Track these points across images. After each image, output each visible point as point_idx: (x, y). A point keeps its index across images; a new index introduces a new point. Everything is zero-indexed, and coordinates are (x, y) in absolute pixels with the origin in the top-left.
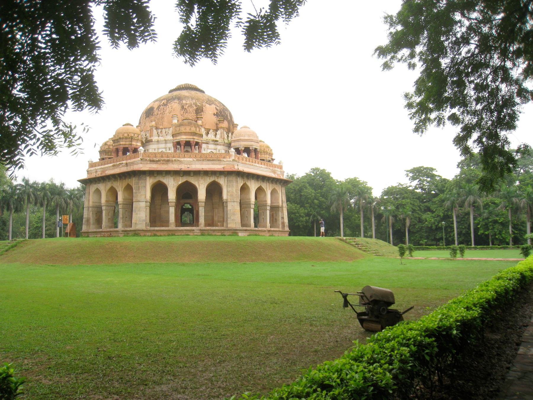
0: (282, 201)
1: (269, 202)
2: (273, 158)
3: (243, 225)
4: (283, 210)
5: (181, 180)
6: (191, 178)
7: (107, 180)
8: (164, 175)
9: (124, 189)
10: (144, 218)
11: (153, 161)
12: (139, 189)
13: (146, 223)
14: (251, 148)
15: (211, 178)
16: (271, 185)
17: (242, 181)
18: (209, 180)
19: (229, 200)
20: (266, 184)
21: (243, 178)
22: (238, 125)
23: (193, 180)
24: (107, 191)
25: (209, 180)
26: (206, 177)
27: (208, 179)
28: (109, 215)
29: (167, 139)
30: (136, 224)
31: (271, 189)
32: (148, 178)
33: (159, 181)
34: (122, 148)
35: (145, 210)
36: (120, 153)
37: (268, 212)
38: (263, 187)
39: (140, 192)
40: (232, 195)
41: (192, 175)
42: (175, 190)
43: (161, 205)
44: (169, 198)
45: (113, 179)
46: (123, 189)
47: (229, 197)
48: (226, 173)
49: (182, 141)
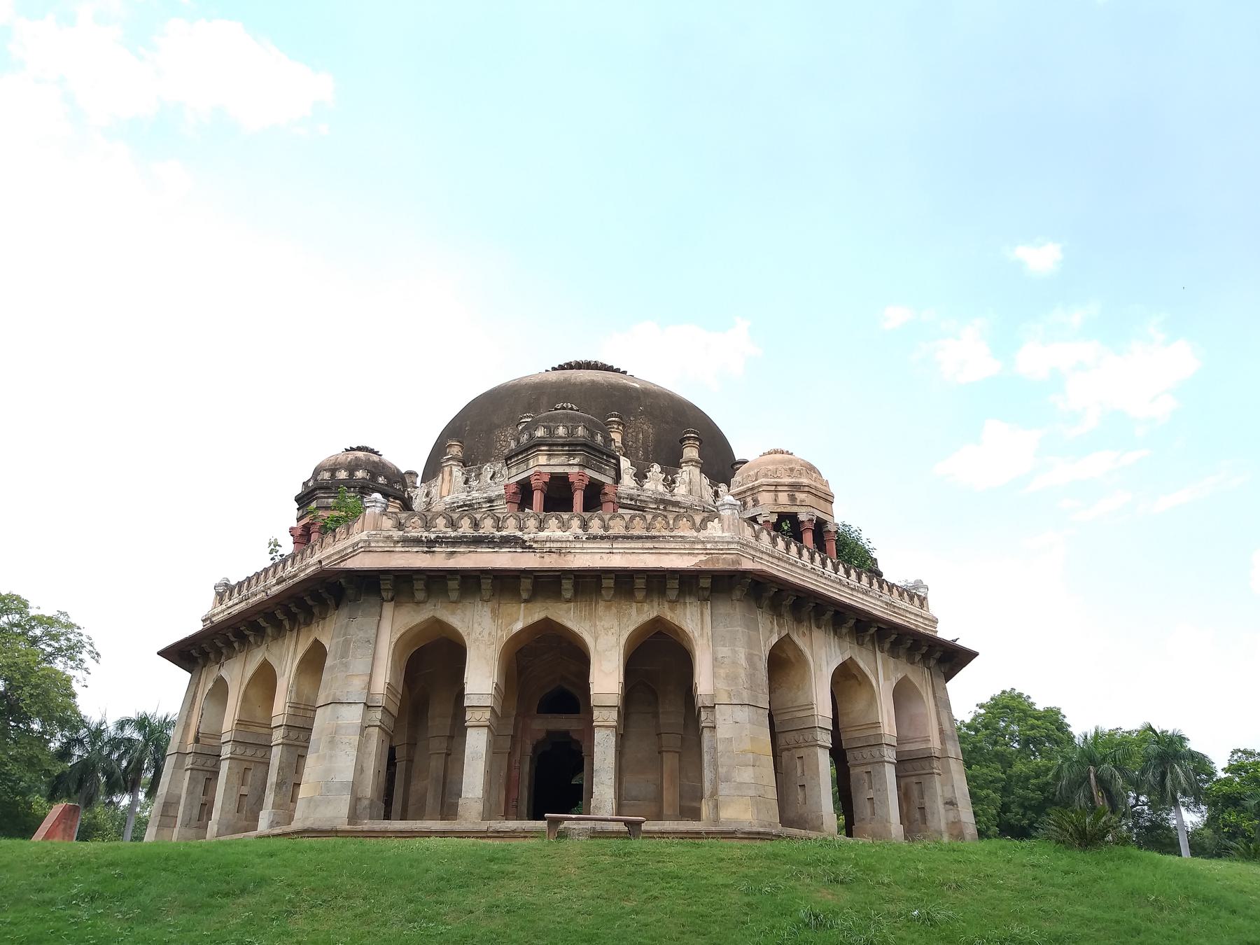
0: (941, 732)
1: (888, 724)
4: (947, 771)
5: (521, 618)
6: (565, 606)
9: (301, 662)
10: (348, 776)
11: (417, 541)
12: (344, 654)
13: (356, 800)
14: (803, 517)
15: (646, 607)
17: (776, 628)
18: (637, 616)
20: (871, 656)
21: (780, 615)
23: (571, 618)
25: (637, 616)
27: (634, 612)
29: (493, 495)
32: (388, 609)
33: (437, 623)
37: (890, 772)
38: (862, 665)
39: (346, 665)
44: (468, 689)
47: (722, 685)
48: (705, 583)
49: (537, 474)
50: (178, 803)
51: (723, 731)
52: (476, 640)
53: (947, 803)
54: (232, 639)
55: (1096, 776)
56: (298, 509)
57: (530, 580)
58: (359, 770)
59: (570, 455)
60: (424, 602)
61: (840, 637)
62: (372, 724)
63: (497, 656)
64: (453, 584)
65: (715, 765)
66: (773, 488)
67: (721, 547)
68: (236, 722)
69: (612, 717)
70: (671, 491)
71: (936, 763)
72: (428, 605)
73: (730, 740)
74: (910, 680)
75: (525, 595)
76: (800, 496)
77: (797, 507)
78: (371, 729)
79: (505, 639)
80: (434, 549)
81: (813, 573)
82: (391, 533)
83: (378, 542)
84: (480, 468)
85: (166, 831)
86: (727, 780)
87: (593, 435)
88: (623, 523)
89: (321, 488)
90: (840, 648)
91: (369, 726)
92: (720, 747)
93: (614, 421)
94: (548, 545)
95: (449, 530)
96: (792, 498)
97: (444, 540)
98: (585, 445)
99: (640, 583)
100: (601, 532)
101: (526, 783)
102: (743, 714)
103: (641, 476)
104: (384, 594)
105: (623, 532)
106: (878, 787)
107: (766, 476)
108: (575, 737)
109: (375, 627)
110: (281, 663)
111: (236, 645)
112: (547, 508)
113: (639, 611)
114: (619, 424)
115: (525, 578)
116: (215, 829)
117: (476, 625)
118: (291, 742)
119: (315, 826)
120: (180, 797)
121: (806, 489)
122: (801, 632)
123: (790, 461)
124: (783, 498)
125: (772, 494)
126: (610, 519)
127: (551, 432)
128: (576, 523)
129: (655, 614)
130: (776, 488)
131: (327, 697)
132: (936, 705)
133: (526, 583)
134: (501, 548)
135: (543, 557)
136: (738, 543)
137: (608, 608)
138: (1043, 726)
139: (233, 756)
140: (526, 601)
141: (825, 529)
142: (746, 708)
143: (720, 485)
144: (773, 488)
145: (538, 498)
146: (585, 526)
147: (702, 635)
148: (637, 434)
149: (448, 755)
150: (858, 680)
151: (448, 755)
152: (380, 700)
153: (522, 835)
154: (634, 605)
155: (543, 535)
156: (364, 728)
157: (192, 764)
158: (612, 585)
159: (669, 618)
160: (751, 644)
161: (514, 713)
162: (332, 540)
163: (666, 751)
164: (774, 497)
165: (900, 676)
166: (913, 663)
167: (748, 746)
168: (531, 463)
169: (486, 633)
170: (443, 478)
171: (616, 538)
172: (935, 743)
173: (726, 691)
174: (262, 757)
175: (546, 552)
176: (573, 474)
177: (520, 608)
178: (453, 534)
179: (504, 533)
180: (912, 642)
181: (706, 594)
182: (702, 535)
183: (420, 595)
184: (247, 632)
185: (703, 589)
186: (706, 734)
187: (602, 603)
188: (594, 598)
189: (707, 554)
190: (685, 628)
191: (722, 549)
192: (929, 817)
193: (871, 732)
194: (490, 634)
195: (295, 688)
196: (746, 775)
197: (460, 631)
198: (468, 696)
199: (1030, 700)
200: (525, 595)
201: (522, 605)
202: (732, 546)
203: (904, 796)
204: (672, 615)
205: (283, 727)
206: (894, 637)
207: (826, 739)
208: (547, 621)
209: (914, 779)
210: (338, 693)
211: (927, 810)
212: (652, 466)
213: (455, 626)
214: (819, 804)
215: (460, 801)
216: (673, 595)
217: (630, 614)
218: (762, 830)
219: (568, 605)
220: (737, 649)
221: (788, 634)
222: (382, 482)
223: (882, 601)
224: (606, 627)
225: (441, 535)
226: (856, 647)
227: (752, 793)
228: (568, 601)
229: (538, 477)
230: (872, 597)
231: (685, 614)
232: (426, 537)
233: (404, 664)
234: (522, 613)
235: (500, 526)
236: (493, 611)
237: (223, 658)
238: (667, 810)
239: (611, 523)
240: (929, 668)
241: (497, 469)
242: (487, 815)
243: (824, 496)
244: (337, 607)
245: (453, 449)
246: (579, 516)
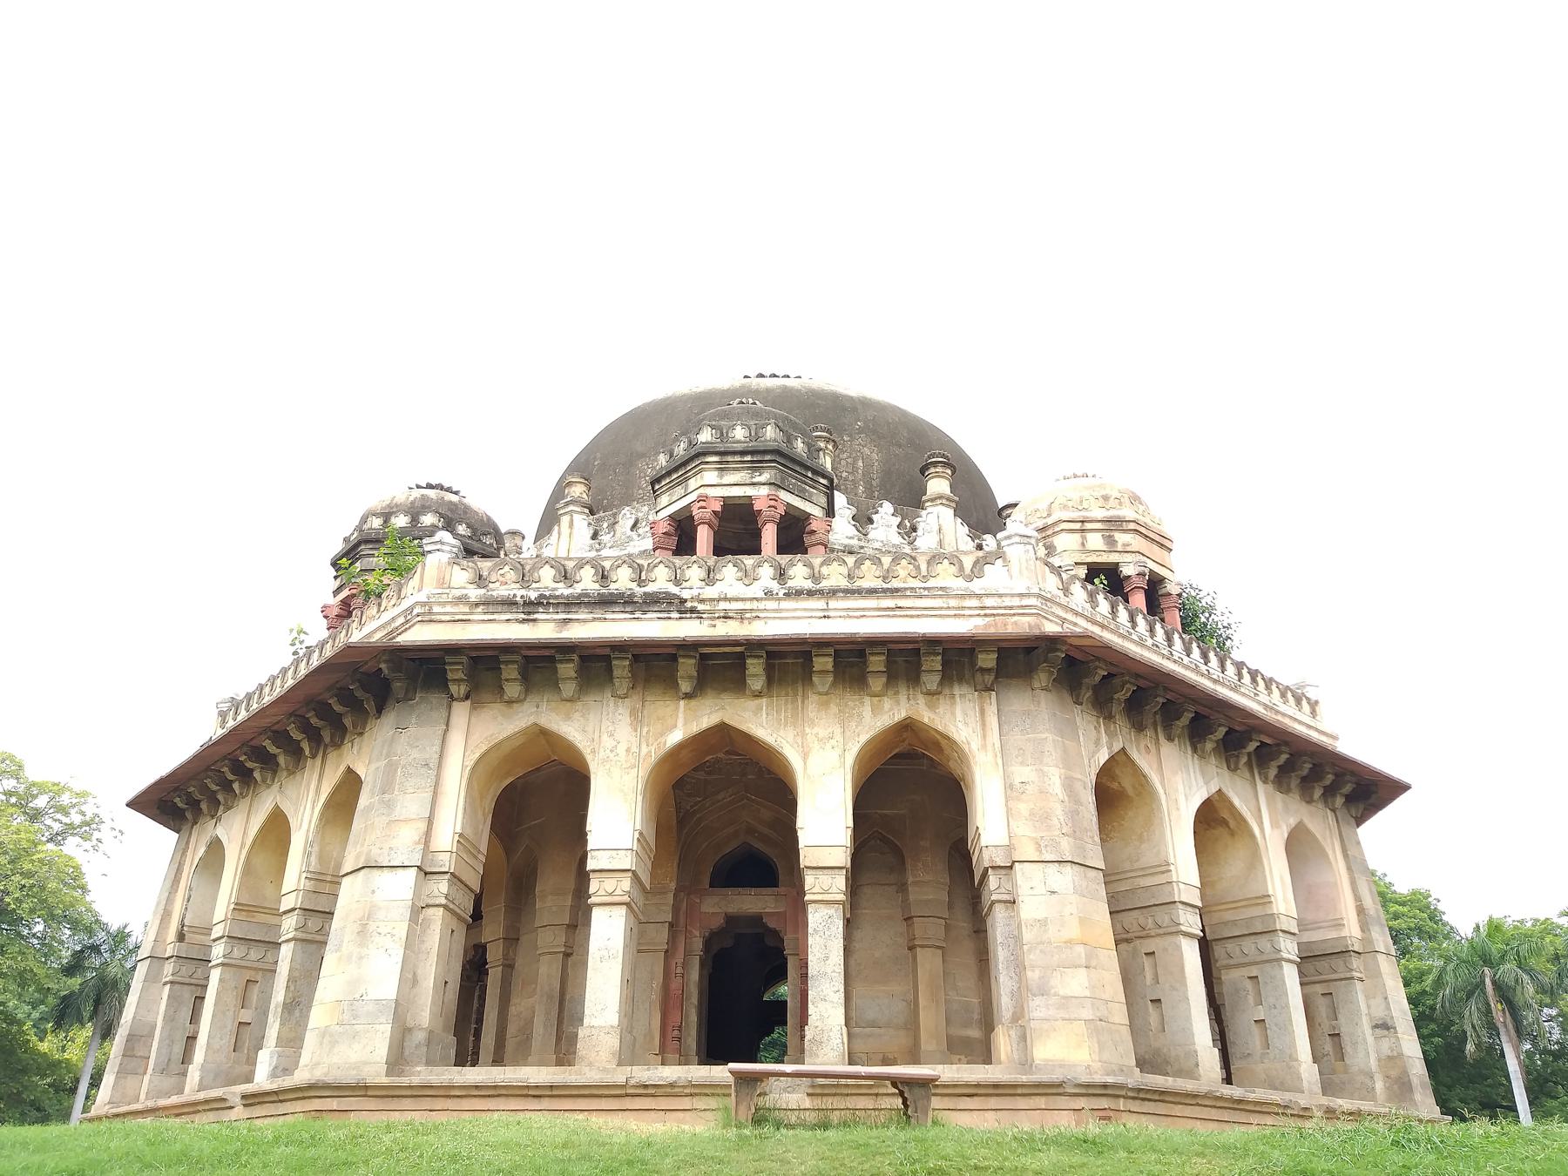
0: (1361, 911)
1: (1283, 902)
3: (1143, 1064)
6: (752, 704)
9: (328, 805)
11: (509, 603)
12: (386, 788)
13: (402, 1033)
14: (1128, 570)
15: (887, 703)
20: (1248, 786)
21: (1109, 717)
24: (249, 842)
26: (851, 699)
27: (867, 710)
30: (324, 1033)
32: (461, 711)
33: (543, 735)
35: (402, 929)
37: (1291, 975)
38: (1237, 802)
39: (389, 805)
47: (1023, 829)
48: (987, 660)
50: (152, 1035)
51: (1030, 908)
52: (606, 760)
54: (230, 777)
55: (1494, 983)
56: (336, 578)
57: (693, 661)
58: (409, 979)
59: (754, 469)
60: (519, 701)
61: (1202, 757)
62: (431, 902)
64: (567, 669)
65: (1019, 967)
66: (1078, 526)
67: (1010, 604)
68: (232, 906)
69: (837, 885)
70: (911, 543)
71: (1355, 962)
72: (526, 705)
73: (1043, 923)
74: (1308, 831)
75: (685, 686)
76: (1122, 538)
77: (1117, 554)
78: (431, 911)
79: (653, 759)
80: (536, 616)
81: (1155, 652)
82: (464, 592)
83: (444, 604)
84: (615, 515)
85: (131, 1081)
86: (1043, 992)
87: (789, 440)
88: (844, 570)
89: (367, 542)
90: (1203, 774)
91: (428, 906)
92: (1027, 936)
93: (820, 437)
94: (723, 605)
95: (561, 585)
96: (1110, 541)
97: (551, 601)
98: (777, 452)
99: (877, 662)
100: (808, 585)
101: (695, 1000)
102: (1065, 879)
103: (863, 520)
104: (453, 688)
105: (843, 583)
106: (1272, 1000)
107: (1065, 507)
108: (772, 924)
109: (438, 742)
110: (296, 811)
111: (236, 786)
112: (719, 551)
113: (876, 711)
114: (828, 440)
115: (684, 656)
116: (197, 1079)
117: (605, 737)
118: (309, 937)
119: (329, 1079)
121: (1132, 526)
122: (1142, 746)
124: (1095, 541)
125: (1077, 536)
126: (822, 564)
127: (722, 435)
128: (766, 572)
129: (903, 715)
130: (1082, 526)
131: (358, 857)
132: (1349, 869)
133: (687, 666)
134: (645, 612)
135: (715, 626)
136: (1039, 596)
137: (826, 705)
138: (1411, 914)
139: (226, 961)
140: (688, 696)
141: (1163, 591)
142: (1068, 867)
143: (985, 537)
144: (1078, 526)
145: (704, 537)
146: (781, 575)
147: (984, 746)
148: (855, 460)
149: (567, 955)
150: (1229, 828)
151: (567, 955)
152: (446, 862)
153: (687, 1091)
154: (867, 700)
155: (710, 592)
156: (418, 910)
157: (172, 975)
158: (830, 667)
159: (926, 720)
160: (1067, 762)
161: (673, 886)
162: (375, 610)
163: (922, 946)
164: (1080, 541)
165: (1293, 821)
166: (1310, 801)
167: (1073, 931)
168: (693, 484)
169: (621, 749)
170: (559, 534)
171: (833, 593)
172: (1352, 929)
174: (241, 959)
175: (718, 618)
177: (677, 709)
178: (567, 592)
179: (651, 588)
180: (1311, 766)
181: (989, 678)
182: (977, 586)
183: (513, 690)
184: (249, 765)
185: (983, 671)
187: (813, 698)
188: (800, 689)
189: (985, 615)
190: (956, 736)
191: (1011, 608)
194: (628, 750)
195: (316, 848)
196: (1075, 983)
198: (594, 853)
199: (1387, 880)
200: (685, 686)
202: (1026, 602)
204: (932, 716)
205: (296, 912)
206: (1284, 757)
208: (722, 730)
210: (375, 851)
211: (1345, 1039)
212: (881, 505)
213: (570, 738)
214: (1188, 1031)
215: (581, 1033)
216: (931, 681)
217: (860, 715)
218: (1110, 1080)
219: (758, 701)
220: (1046, 769)
222: (463, 533)
223: (1259, 703)
224: (820, 736)
225: (547, 593)
226: (1226, 772)
227: (1087, 1014)
229: (702, 504)
230: (1244, 695)
231: (953, 714)
232: (522, 597)
233: (489, 805)
234: (681, 715)
235: (643, 577)
236: (633, 713)
237: (221, 808)
238: (927, 1044)
239: (825, 570)
240: (1334, 811)
241: (640, 515)
242: (628, 1055)
243: (1157, 538)
244: (380, 711)
245: (573, 489)
246: (770, 560)
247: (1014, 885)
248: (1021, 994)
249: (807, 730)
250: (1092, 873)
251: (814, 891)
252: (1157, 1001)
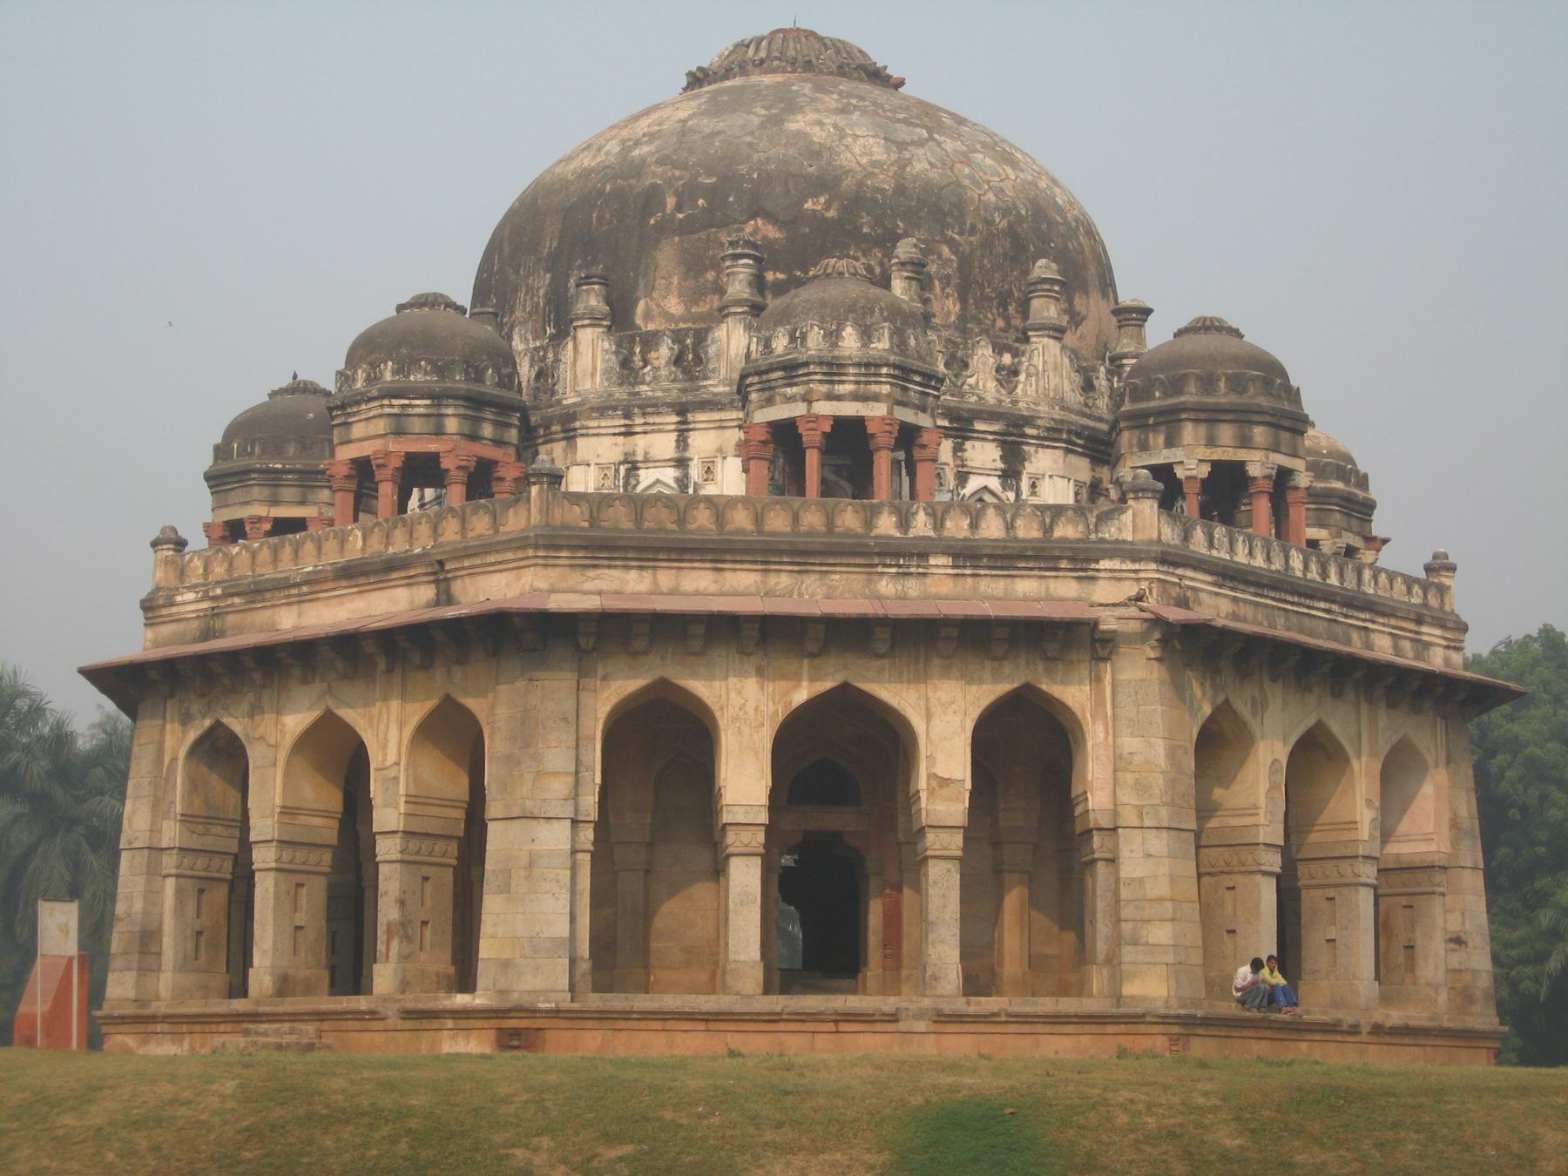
2: (1377, 529)
7: (296, 671)
8: (697, 645)
10: (562, 929)
14: (1254, 470)
15: (1007, 668)
16: (1383, 719)
19: (1129, 817)
22: (1147, 312)
28: (296, 908)
31: (1386, 742)
33: (663, 683)
34: (397, 462)
36: (387, 492)
37: (1365, 898)
40: (1141, 788)
41: (882, 648)
42: (764, 740)
43: (651, 845)
45: (340, 665)
46: (408, 731)
51: (1131, 867)
53: (1451, 940)
60: (646, 653)
63: (768, 745)
69: (955, 842)
73: (1141, 881)
79: (780, 718)
92: (1125, 893)
104: (583, 642)
117: (733, 695)
118: (412, 858)
120: (161, 923)
123: (1235, 359)
140: (811, 656)
141: (1292, 483)
142: (1164, 834)
154: (988, 664)
163: (1009, 871)
165: (1395, 739)
169: (750, 707)
170: (575, 348)
173: (1136, 806)
176: (873, 419)
186: (1101, 868)
192: (1420, 962)
193: (1344, 836)
194: (756, 709)
197: (707, 701)
198: (730, 808)
201: (806, 662)
203: (1382, 927)
206: (1391, 679)
207: (1273, 862)
209: (1404, 901)
210: (529, 803)
218: (1182, 1012)
219: (879, 662)
221: (1227, 701)
227: (1170, 959)
228: (879, 656)
247: (1117, 846)
248: (1117, 940)
249: (930, 694)
250: (1185, 835)
251: (935, 847)
252: (1232, 932)
